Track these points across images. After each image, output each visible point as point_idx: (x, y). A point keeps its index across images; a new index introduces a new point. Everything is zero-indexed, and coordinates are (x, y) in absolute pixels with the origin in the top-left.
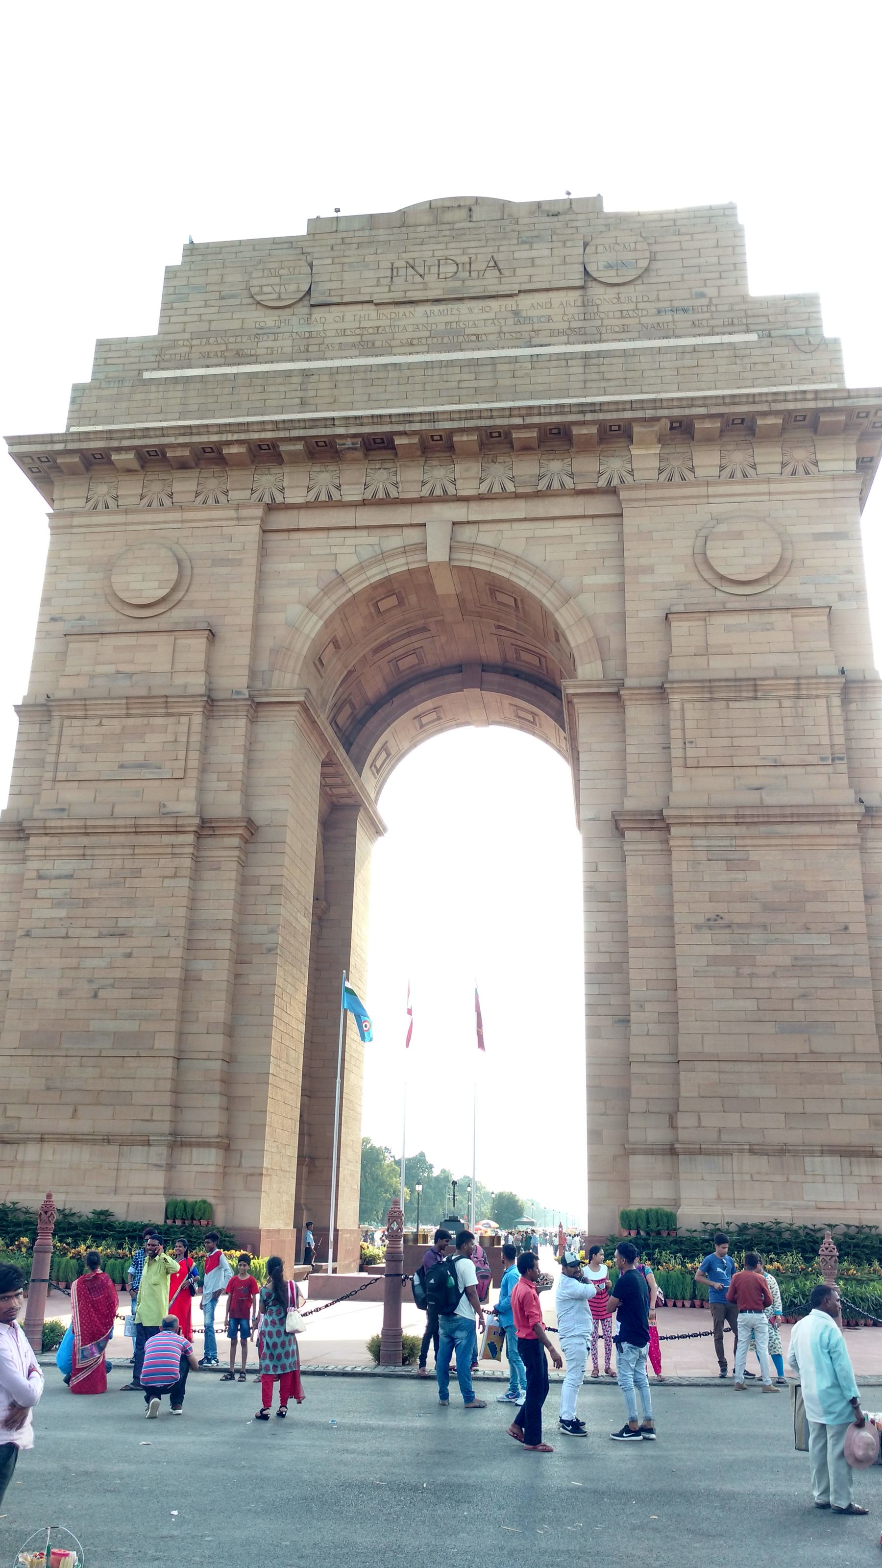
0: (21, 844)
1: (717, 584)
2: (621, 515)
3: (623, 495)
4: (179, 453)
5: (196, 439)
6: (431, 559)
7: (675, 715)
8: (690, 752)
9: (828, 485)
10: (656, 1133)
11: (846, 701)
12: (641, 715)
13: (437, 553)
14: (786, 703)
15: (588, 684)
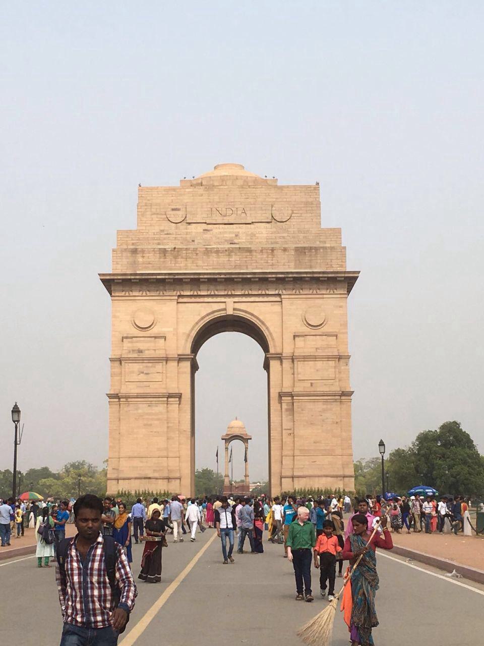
0: (117, 400)
1: (307, 325)
2: (281, 302)
3: (283, 297)
4: (152, 280)
5: (158, 277)
6: (228, 314)
7: (296, 365)
8: (299, 376)
9: (339, 296)
10: (289, 474)
11: (339, 361)
12: (287, 364)
13: (230, 312)
14: (324, 362)
15: (272, 354)
